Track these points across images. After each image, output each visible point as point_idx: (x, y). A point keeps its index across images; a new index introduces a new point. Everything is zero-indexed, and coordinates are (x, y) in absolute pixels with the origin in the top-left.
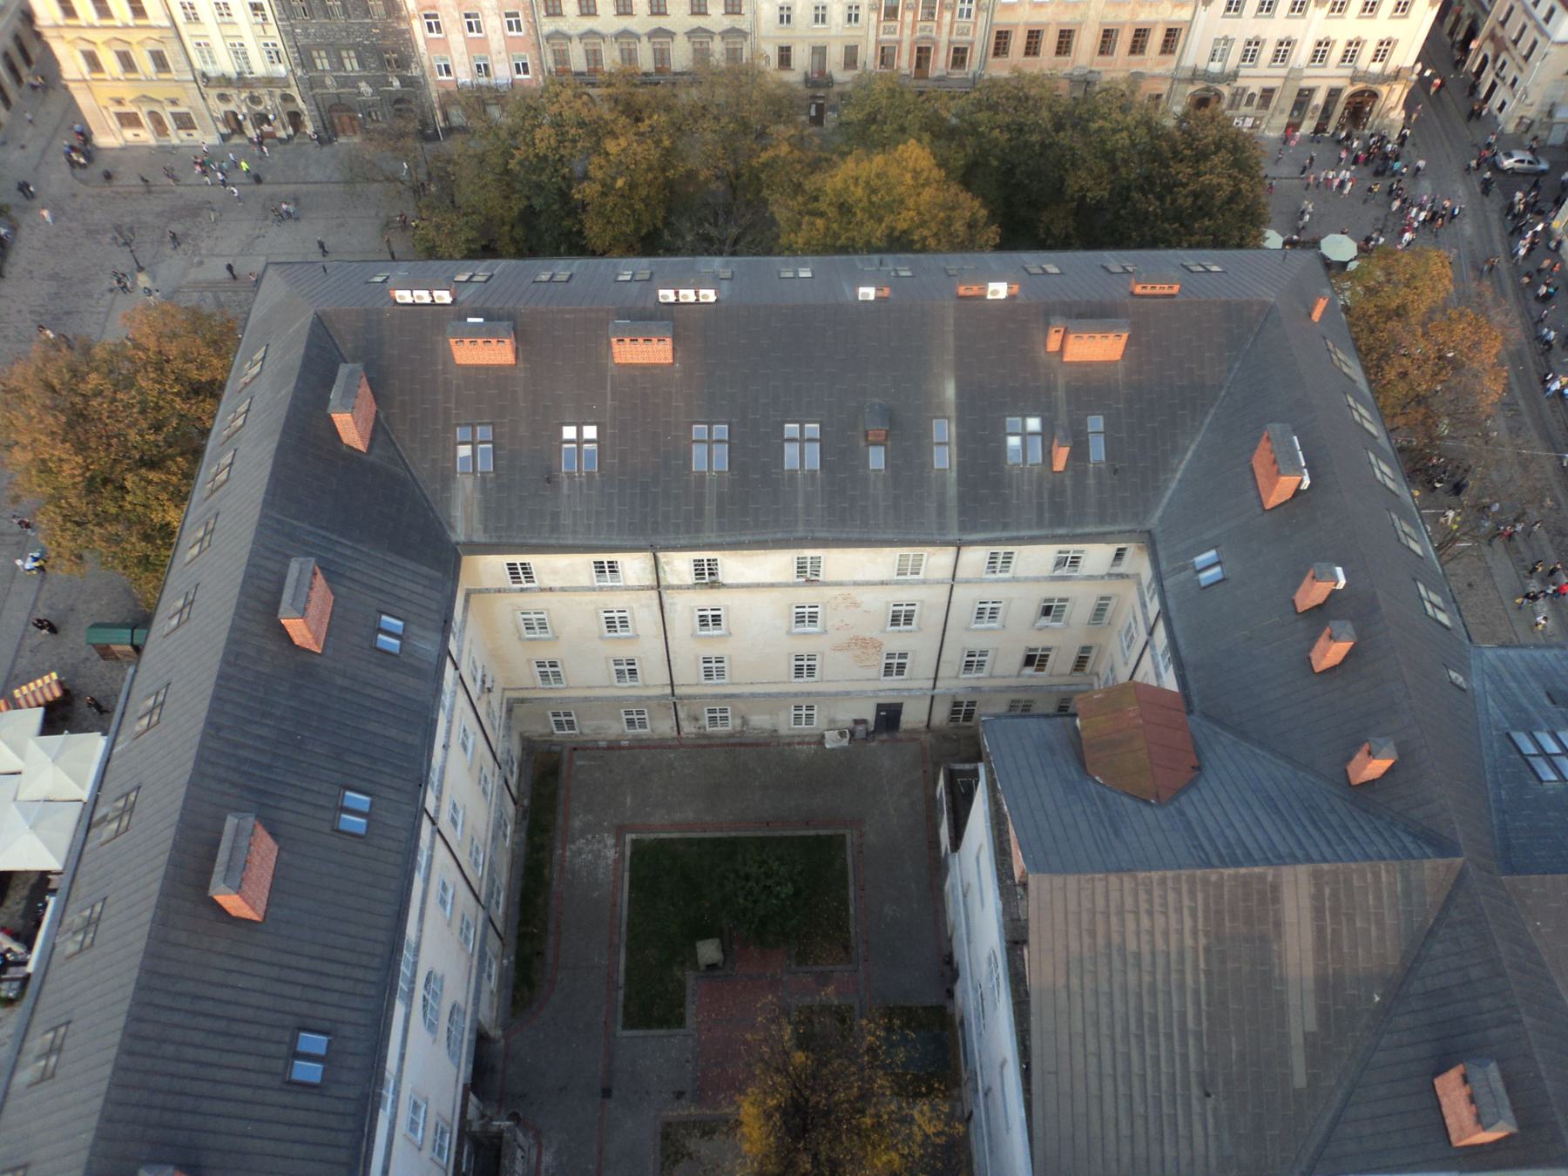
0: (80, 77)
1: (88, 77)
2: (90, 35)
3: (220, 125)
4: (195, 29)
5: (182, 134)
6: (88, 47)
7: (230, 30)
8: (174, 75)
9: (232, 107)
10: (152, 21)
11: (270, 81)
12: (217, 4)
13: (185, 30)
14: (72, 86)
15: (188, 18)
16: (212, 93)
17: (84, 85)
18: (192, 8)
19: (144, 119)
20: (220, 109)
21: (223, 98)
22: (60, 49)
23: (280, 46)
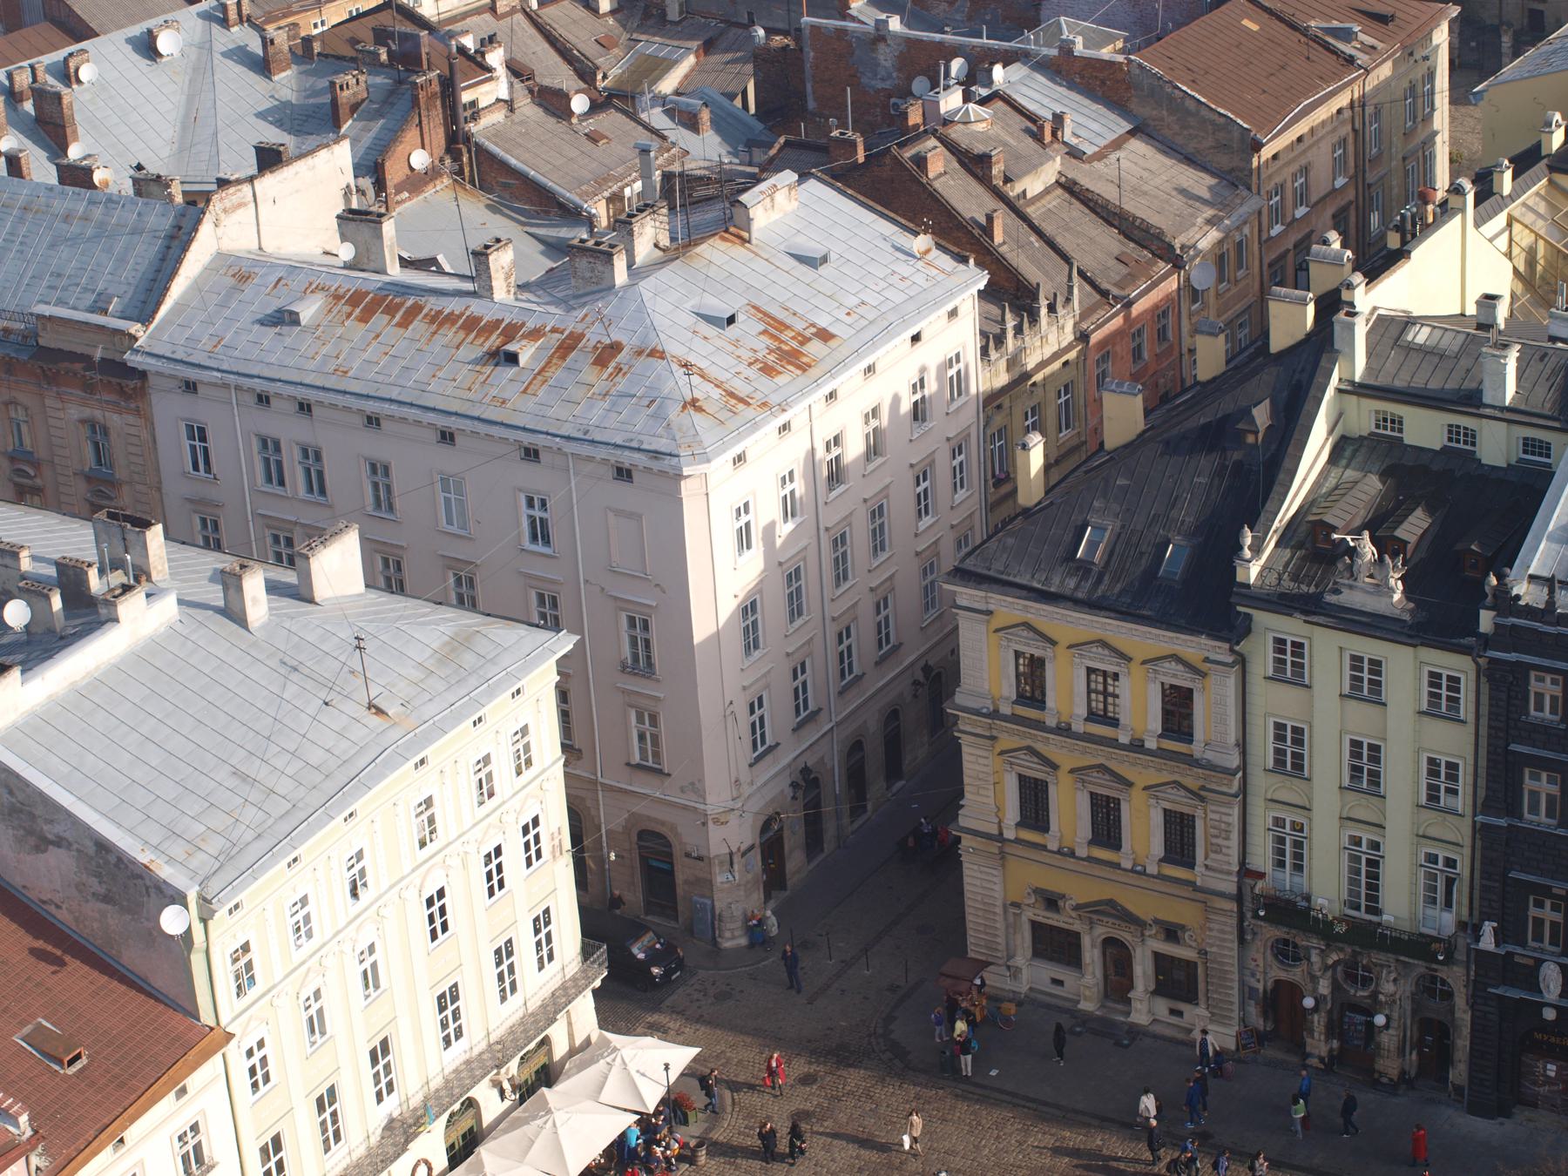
0: (995, 832)
1: (1010, 834)
2: (1053, 748)
3: (1253, 1010)
4: (1288, 790)
5: (1162, 1006)
6: (1036, 771)
7: (1363, 808)
8: (1199, 875)
9: (1296, 974)
10: (1197, 748)
11: (1417, 946)
12: (1356, 744)
13: (1263, 784)
14: (967, 842)
15: (1280, 762)
16: (1272, 932)
17: (994, 847)
18: (1298, 742)
19: (1091, 954)
20: (1269, 969)
21: (1286, 952)
22: (976, 762)
23: (1463, 868)
